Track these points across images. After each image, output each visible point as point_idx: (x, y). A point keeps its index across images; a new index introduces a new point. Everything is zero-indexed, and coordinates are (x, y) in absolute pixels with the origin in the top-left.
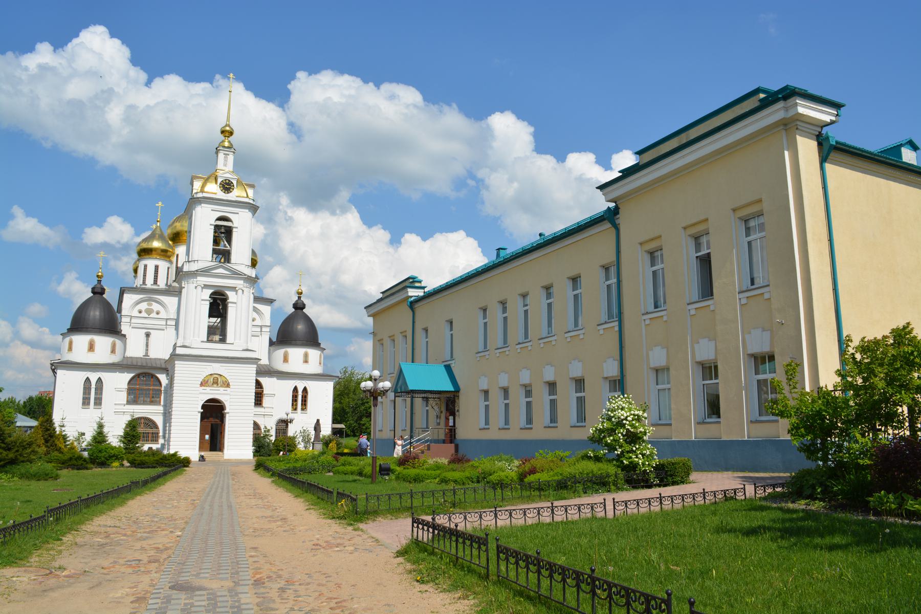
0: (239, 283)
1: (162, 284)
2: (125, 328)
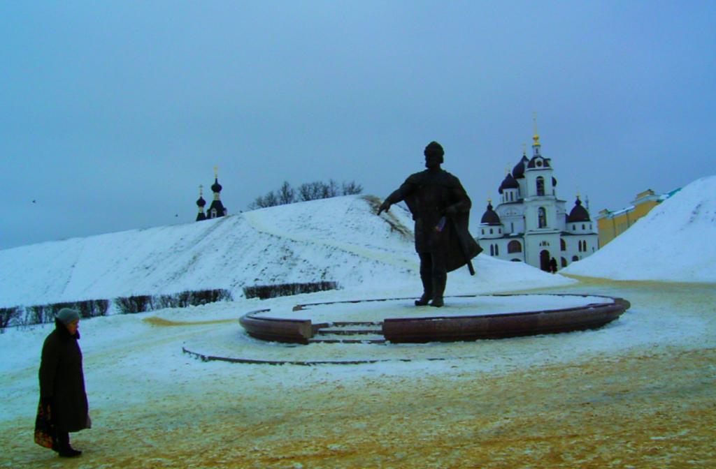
0: (549, 203)
1: (515, 200)
2: (502, 222)
